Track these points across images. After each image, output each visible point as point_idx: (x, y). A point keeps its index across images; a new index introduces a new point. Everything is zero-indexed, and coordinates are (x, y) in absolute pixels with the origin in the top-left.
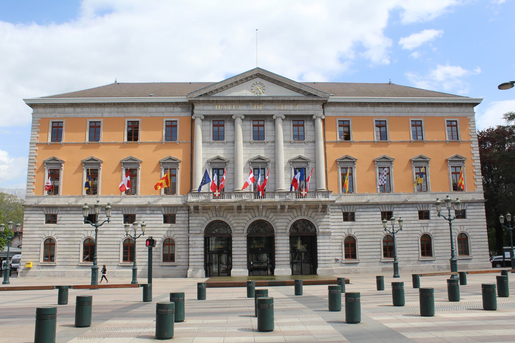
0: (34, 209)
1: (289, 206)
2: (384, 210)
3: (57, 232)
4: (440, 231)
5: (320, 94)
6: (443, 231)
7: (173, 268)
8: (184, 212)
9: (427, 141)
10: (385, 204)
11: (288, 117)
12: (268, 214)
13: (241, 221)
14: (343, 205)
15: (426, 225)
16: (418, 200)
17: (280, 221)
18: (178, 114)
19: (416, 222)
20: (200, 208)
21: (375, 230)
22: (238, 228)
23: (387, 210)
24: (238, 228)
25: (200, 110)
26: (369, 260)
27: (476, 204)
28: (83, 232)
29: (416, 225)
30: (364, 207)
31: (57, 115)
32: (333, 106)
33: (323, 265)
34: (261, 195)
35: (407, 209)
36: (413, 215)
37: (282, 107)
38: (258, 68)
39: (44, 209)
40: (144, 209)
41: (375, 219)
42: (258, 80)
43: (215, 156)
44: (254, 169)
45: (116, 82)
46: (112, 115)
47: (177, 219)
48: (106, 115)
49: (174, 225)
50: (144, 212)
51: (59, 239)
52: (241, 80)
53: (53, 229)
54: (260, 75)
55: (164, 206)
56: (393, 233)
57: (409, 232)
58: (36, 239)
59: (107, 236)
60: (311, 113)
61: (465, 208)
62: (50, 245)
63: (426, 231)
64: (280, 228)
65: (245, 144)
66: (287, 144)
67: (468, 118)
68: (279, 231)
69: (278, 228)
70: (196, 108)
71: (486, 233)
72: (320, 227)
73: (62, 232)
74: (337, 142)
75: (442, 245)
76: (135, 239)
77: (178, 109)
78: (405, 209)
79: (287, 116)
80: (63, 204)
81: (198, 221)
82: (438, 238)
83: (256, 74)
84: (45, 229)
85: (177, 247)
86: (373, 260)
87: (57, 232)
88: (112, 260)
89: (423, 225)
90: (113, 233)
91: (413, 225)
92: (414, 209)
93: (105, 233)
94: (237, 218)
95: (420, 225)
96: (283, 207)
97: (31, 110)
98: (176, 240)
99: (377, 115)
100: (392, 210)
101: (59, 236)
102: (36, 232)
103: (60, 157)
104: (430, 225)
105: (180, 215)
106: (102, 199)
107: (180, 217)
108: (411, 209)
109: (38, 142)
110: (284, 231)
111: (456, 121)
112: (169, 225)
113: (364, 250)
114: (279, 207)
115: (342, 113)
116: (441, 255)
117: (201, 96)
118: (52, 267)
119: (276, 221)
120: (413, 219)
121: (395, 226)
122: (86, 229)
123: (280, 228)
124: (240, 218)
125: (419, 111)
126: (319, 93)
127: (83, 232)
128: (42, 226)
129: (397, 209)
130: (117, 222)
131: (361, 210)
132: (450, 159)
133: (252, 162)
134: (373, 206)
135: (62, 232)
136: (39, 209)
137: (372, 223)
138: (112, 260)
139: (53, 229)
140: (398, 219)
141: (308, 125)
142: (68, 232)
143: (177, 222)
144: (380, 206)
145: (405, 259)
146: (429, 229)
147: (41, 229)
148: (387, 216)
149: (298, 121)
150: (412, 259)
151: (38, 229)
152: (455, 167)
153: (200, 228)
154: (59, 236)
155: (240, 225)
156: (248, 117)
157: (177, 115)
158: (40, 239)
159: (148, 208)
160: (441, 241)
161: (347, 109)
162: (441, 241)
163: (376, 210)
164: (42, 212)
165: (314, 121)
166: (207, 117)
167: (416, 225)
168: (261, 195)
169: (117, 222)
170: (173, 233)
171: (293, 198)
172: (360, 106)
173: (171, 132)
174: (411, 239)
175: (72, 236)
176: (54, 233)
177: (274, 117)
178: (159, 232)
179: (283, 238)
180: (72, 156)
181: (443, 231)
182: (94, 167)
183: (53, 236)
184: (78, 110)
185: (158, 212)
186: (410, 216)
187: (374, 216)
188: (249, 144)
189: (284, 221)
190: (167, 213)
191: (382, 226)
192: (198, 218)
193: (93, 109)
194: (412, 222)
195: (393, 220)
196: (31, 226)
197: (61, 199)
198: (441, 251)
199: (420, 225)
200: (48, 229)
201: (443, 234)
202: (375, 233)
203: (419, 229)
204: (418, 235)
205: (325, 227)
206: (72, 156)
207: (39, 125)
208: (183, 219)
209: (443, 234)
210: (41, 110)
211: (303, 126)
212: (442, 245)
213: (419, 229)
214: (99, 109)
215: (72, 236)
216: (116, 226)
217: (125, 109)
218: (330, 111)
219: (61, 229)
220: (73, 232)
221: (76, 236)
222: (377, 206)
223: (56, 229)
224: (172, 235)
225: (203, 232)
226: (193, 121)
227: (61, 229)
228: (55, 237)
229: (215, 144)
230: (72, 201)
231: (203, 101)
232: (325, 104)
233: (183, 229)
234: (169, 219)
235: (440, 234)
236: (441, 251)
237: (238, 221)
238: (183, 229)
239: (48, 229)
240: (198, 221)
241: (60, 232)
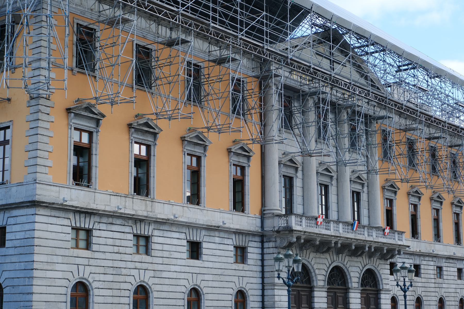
0: (54, 213)
1: (387, 250)
3: (93, 269)
39: (71, 216)
49: (246, 267)
53: (85, 262)
59: (167, 281)
73: (102, 270)
87: (93, 269)
90: (174, 275)
93: (165, 275)
107: (253, 253)
122: (138, 265)
128: (67, 252)
135: (102, 270)
139: (85, 262)
147: (66, 260)
151: (60, 259)
159: (217, 234)
168: (355, 229)
178: (228, 278)
200: (78, 261)
223: (92, 262)
228: (90, 280)
239: (78, 261)
241: (98, 270)
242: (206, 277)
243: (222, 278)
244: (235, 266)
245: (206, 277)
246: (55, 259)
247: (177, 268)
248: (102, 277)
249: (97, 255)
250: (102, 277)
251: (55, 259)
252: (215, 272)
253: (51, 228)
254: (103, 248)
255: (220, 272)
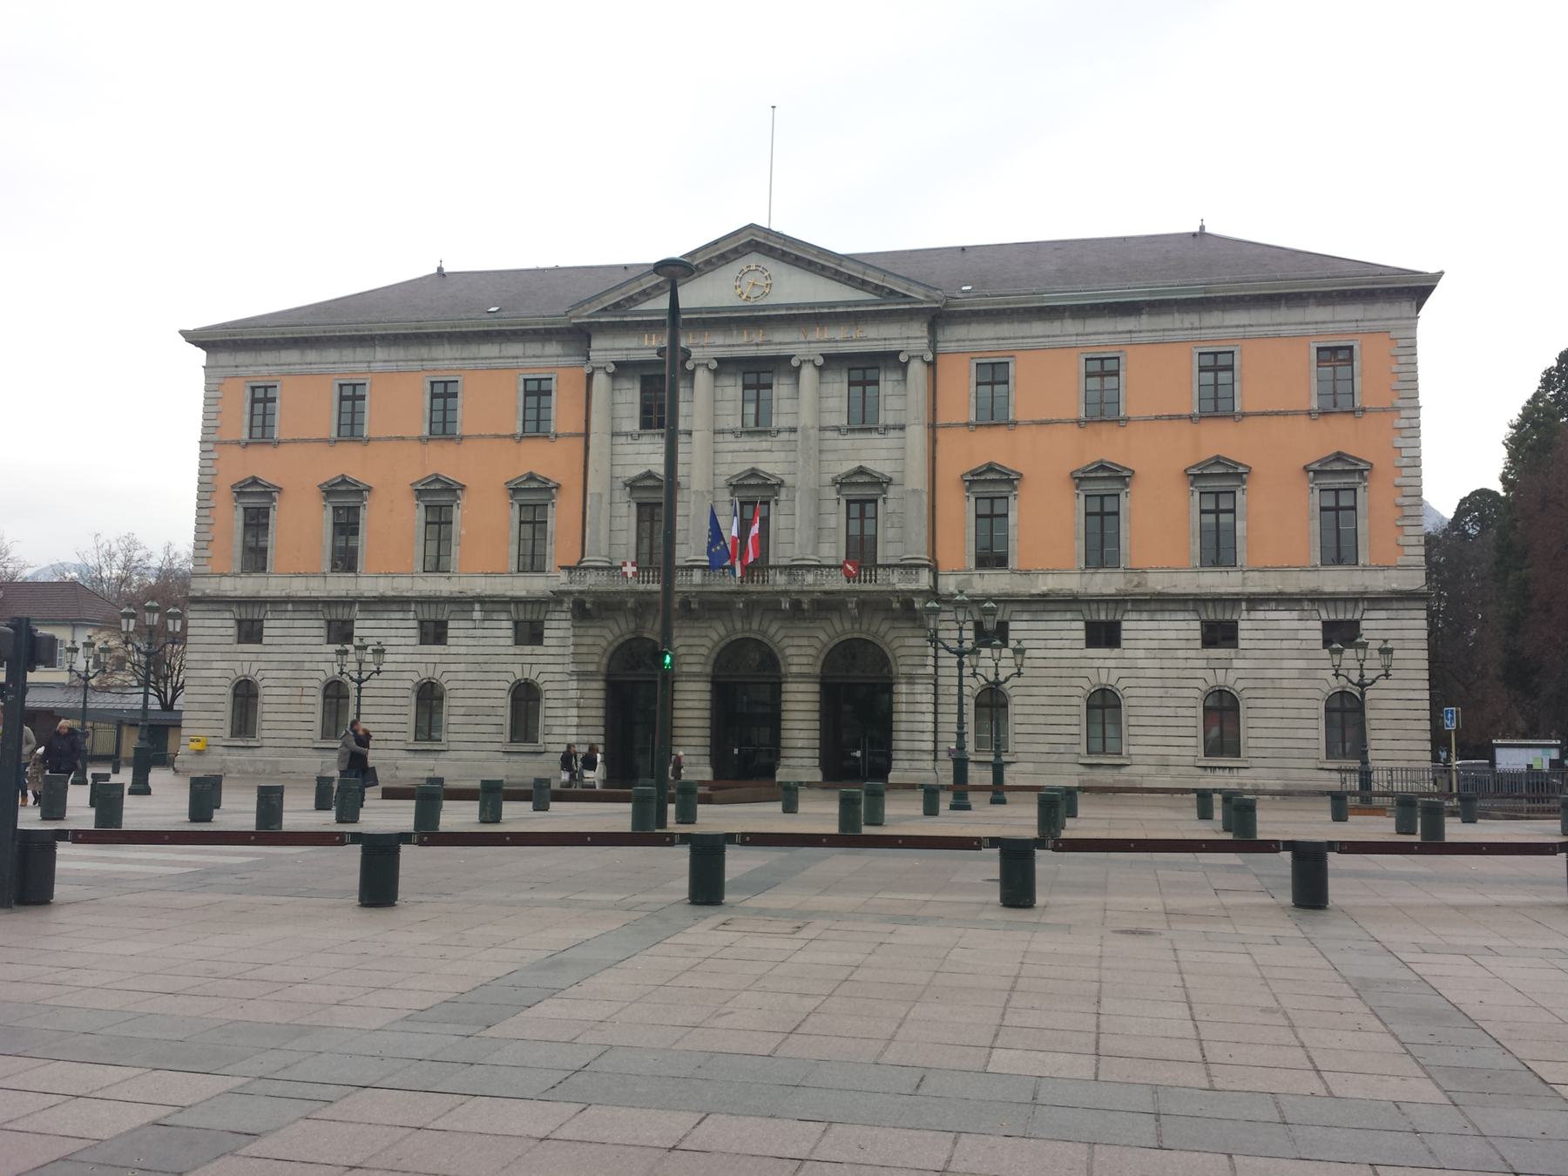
0: (211, 607)
2: (1095, 618)
3: (263, 665)
4: (1267, 683)
5: (918, 293)
6: (1277, 684)
7: (533, 757)
8: (563, 616)
9: (1244, 415)
10: (1098, 601)
11: (832, 361)
12: (766, 624)
13: (697, 641)
14: (976, 601)
15: (1224, 664)
16: (1328, 588)
17: (797, 642)
18: (548, 359)
19: (1076, 653)
20: (588, 606)
21: (1065, 672)
22: (690, 659)
23: (1103, 617)
24: (690, 659)
25: (606, 350)
26: (1044, 758)
27: (1396, 605)
28: (322, 666)
29: (1190, 663)
30: (1034, 607)
31: (261, 367)
32: (964, 323)
33: (906, 765)
34: (738, 574)
35: (1167, 616)
36: (1182, 635)
37: (817, 334)
38: (752, 226)
40: (467, 607)
41: (1067, 644)
42: (754, 259)
43: (644, 470)
44: (742, 504)
45: (440, 269)
46: (392, 366)
47: (546, 633)
48: (377, 366)
49: (538, 649)
50: (466, 616)
51: (265, 682)
52: (708, 262)
53: (253, 657)
54: (756, 244)
55: (517, 601)
56: (1362, 685)
57: (1169, 683)
58: (215, 682)
60: (895, 346)
61: (1358, 616)
62: (245, 695)
63: (1221, 681)
64: (796, 660)
65: (720, 438)
66: (829, 434)
67: (1394, 334)
68: (794, 669)
69: (790, 660)
70: (595, 344)
71: (1426, 695)
72: (900, 661)
74: (967, 424)
75: (1272, 723)
76: (360, 682)
77: (553, 348)
78: (1158, 616)
79: (828, 358)
80: (277, 594)
81: (589, 641)
82: (1259, 703)
83: (749, 244)
84: (233, 657)
85: (544, 704)
86: (1054, 758)
87: (263, 665)
88: (388, 736)
89: (1214, 664)
91: (1182, 664)
92: (1188, 616)
94: (687, 632)
95: (1203, 663)
96: (796, 605)
97: (200, 355)
98: (544, 687)
99: (1095, 339)
100: (1118, 617)
101: (268, 674)
102: (215, 665)
103: (268, 477)
104: (1236, 663)
105: (554, 624)
106: (367, 585)
108: (1181, 616)
109: (215, 438)
110: (805, 670)
111: (1351, 348)
112: (527, 649)
113: (1030, 729)
114: (786, 605)
115: (986, 338)
116: (1268, 753)
117: (605, 309)
118: (250, 752)
119: (787, 642)
120: (1182, 644)
121: (1367, 664)
123: (796, 660)
124: (695, 632)
125: (1227, 323)
126: (915, 288)
127: (322, 666)
128: (228, 648)
129: (1134, 616)
130: (403, 641)
131: (1025, 616)
132: (1316, 467)
133: (735, 487)
134: (1062, 606)
135: (274, 665)
136: (223, 607)
137: (1057, 654)
138: (388, 736)
140: (1379, 644)
141: (888, 383)
142: (289, 666)
143: (546, 642)
144: (1084, 607)
145: (1151, 760)
146: (1232, 675)
147: (227, 657)
148: (1104, 635)
149: (864, 370)
150: (1173, 760)
152: (1337, 491)
153: (596, 659)
154: (268, 674)
155: (694, 650)
156: (725, 366)
157: (553, 362)
158: (222, 682)
160: (1269, 713)
161: (1005, 329)
162: (1269, 713)
163: (1069, 616)
164: (228, 615)
165: (904, 367)
166: (622, 369)
167: (1190, 663)
168: (738, 574)
169: (403, 641)
170: (536, 669)
171: (836, 582)
172: (1040, 319)
173: (539, 408)
174: (1172, 702)
175: (297, 674)
176: (256, 666)
177: (795, 363)
179: (802, 687)
180: (299, 475)
181: (1277, 684)
182: (350, 501)
183: (253, 673)
184: (312, 355)
185: (504, 616)
186: (1172, 635)
187: (1064, 634)
188: (730, 437)
189: (804, 642)
190: (522, 617)
191: (1328, 664)
192: (591, 631)
193: (348, 354)
194: (1181, 654)
195: (1364, 646)
196: (206, 648)
197: (273, 582)
198: (1270, 743)
199: (1203, 663)
200: (242, 657)
201: (1278, 693)
202: (1065, 682)
203: (1200, 673)
204: (1196, 693)
205: (917, 660)
206: (299, 475)
207: (219, 394)
208: (560, 633)
209: (1278, 693)
210: (224, 358)
211: (876, 383)
212: (1272, 723)
213: (1200, 673)
214: (361, 353)
215: (297, 674)
216: (401, 649)
217: (424, 352)
218: (955, 337)
219: (272, 657)
220: (298, 666)
221: (306, 674)
222: (1074, 607)
224: (533, 677)
225: (603, 669)
226: (590, 377)
227: (272, 657)
228: (258, 677)
229: (644, 439)
230: (299, 588)
231: (613, 324)
232: (938, 318)
233: (560, 660)
234: (529, 633)
235: (1269, 693)
236: (1270, 743)
237: (690, 641)
238: (560, 660)
239: (242, 657)
240: (589, 641)
242: (453, 667)
243: (486, 667)
244: (517, 650)
245: (453, 667)
246: (213, 656)
247: (400, 658)
248: (275, 674)
249: (268, 649)
250: (275, 674)
251: (213, 656)
252: (472, 659)
253: (208, 623)
254: (276, 640)
255: (481, 659)
